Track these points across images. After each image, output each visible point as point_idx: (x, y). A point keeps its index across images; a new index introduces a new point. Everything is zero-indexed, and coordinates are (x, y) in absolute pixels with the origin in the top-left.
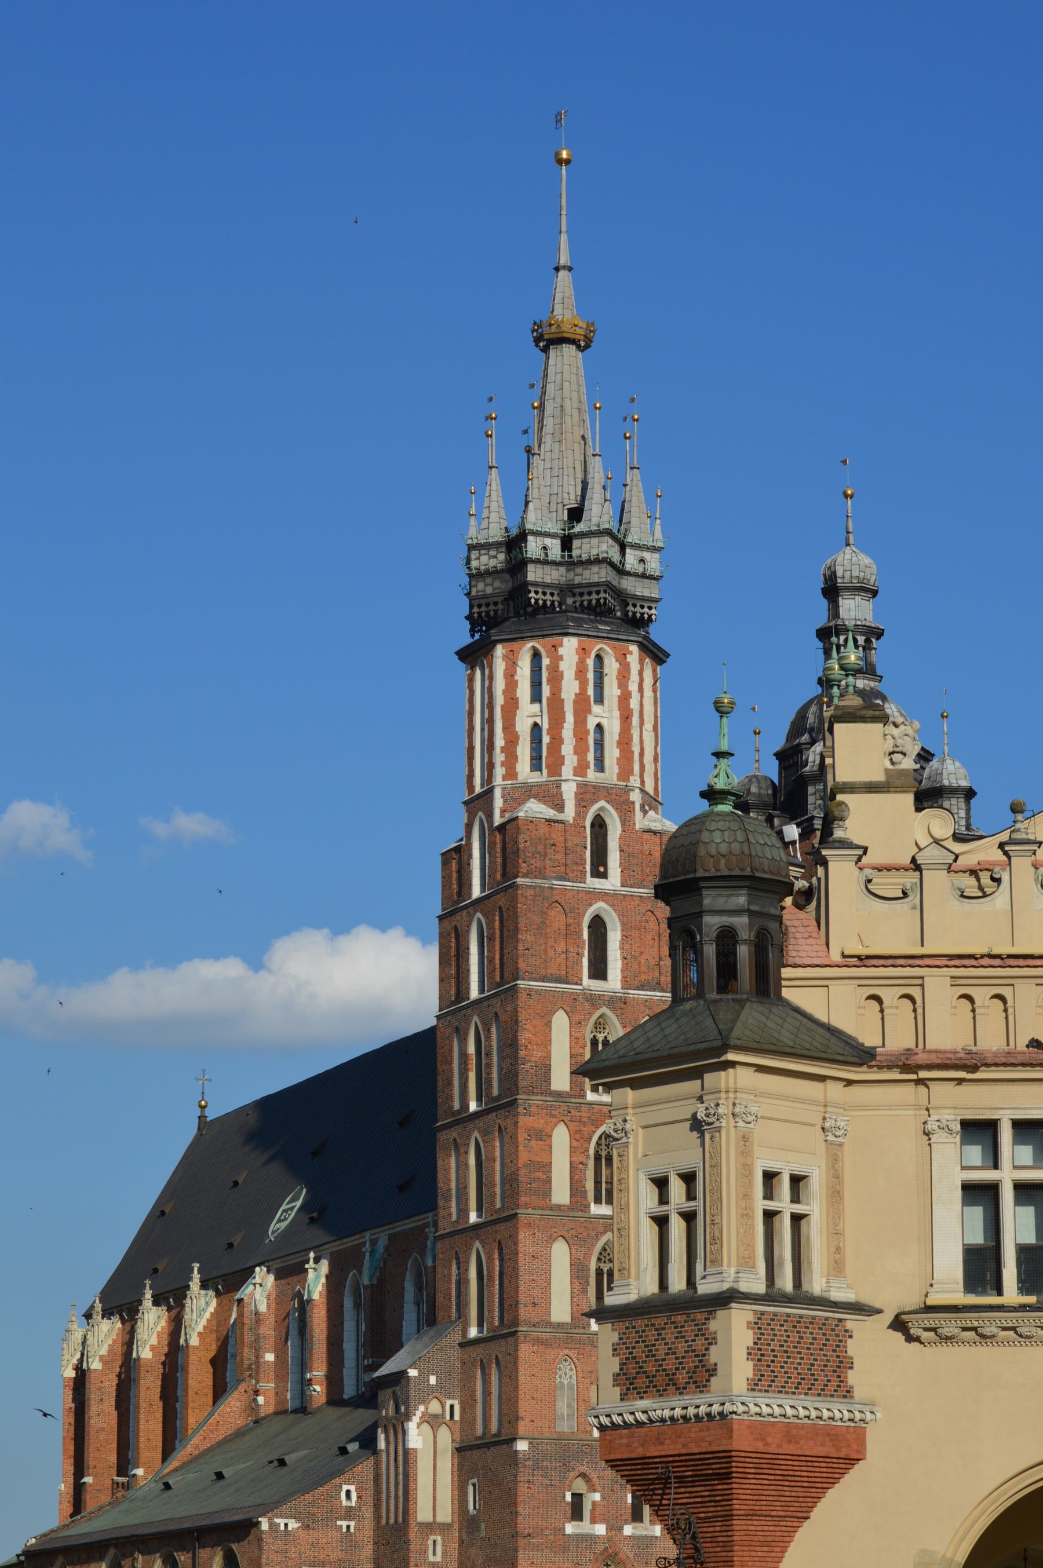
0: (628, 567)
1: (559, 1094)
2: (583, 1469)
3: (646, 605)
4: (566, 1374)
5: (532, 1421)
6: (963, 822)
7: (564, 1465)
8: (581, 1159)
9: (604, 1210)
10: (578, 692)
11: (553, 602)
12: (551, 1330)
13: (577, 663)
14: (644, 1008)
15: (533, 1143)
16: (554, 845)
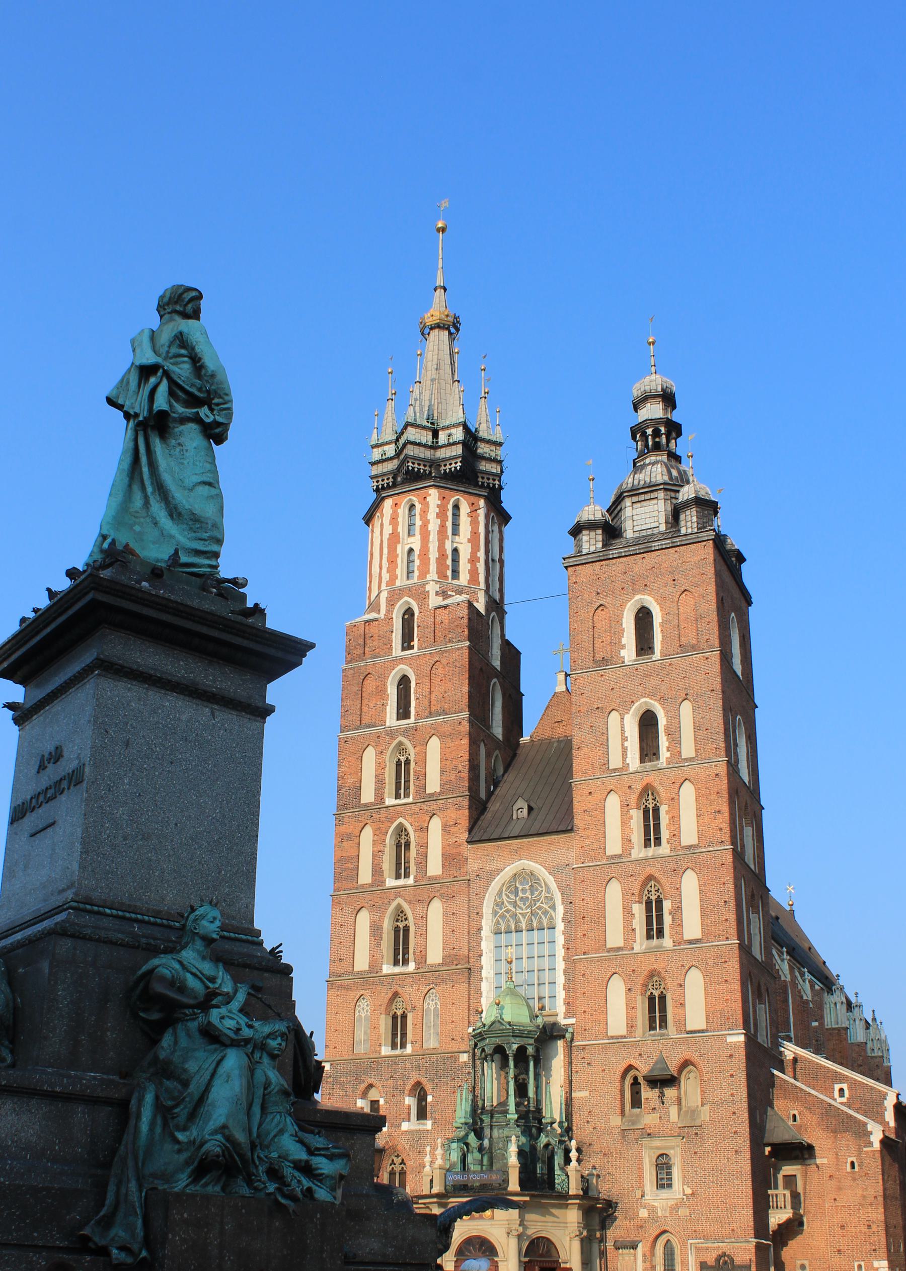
0: (440, 444)
1: (366, 805)
2: (371, 1081)
3: (453, 462)
4: (363, 1010)
5: (335, 1048)
6: (695, 525)
7: (356, 1079)
8: (379, 848)
9: (401, 882)
10: (391, 532)
11: (388, 484)
12: (351, 977)
13: (391, 515)
14: (430, 730)
15: (345, 844)
16: (371, 637)
